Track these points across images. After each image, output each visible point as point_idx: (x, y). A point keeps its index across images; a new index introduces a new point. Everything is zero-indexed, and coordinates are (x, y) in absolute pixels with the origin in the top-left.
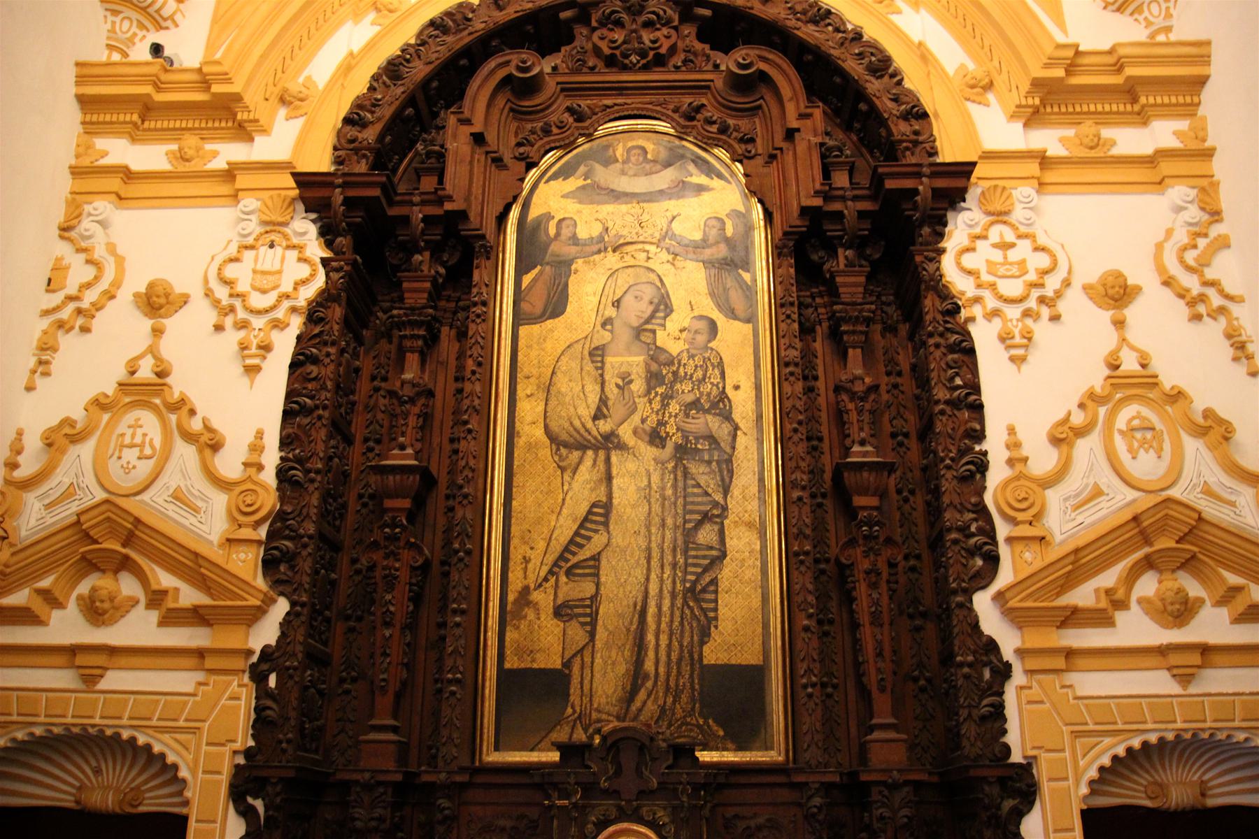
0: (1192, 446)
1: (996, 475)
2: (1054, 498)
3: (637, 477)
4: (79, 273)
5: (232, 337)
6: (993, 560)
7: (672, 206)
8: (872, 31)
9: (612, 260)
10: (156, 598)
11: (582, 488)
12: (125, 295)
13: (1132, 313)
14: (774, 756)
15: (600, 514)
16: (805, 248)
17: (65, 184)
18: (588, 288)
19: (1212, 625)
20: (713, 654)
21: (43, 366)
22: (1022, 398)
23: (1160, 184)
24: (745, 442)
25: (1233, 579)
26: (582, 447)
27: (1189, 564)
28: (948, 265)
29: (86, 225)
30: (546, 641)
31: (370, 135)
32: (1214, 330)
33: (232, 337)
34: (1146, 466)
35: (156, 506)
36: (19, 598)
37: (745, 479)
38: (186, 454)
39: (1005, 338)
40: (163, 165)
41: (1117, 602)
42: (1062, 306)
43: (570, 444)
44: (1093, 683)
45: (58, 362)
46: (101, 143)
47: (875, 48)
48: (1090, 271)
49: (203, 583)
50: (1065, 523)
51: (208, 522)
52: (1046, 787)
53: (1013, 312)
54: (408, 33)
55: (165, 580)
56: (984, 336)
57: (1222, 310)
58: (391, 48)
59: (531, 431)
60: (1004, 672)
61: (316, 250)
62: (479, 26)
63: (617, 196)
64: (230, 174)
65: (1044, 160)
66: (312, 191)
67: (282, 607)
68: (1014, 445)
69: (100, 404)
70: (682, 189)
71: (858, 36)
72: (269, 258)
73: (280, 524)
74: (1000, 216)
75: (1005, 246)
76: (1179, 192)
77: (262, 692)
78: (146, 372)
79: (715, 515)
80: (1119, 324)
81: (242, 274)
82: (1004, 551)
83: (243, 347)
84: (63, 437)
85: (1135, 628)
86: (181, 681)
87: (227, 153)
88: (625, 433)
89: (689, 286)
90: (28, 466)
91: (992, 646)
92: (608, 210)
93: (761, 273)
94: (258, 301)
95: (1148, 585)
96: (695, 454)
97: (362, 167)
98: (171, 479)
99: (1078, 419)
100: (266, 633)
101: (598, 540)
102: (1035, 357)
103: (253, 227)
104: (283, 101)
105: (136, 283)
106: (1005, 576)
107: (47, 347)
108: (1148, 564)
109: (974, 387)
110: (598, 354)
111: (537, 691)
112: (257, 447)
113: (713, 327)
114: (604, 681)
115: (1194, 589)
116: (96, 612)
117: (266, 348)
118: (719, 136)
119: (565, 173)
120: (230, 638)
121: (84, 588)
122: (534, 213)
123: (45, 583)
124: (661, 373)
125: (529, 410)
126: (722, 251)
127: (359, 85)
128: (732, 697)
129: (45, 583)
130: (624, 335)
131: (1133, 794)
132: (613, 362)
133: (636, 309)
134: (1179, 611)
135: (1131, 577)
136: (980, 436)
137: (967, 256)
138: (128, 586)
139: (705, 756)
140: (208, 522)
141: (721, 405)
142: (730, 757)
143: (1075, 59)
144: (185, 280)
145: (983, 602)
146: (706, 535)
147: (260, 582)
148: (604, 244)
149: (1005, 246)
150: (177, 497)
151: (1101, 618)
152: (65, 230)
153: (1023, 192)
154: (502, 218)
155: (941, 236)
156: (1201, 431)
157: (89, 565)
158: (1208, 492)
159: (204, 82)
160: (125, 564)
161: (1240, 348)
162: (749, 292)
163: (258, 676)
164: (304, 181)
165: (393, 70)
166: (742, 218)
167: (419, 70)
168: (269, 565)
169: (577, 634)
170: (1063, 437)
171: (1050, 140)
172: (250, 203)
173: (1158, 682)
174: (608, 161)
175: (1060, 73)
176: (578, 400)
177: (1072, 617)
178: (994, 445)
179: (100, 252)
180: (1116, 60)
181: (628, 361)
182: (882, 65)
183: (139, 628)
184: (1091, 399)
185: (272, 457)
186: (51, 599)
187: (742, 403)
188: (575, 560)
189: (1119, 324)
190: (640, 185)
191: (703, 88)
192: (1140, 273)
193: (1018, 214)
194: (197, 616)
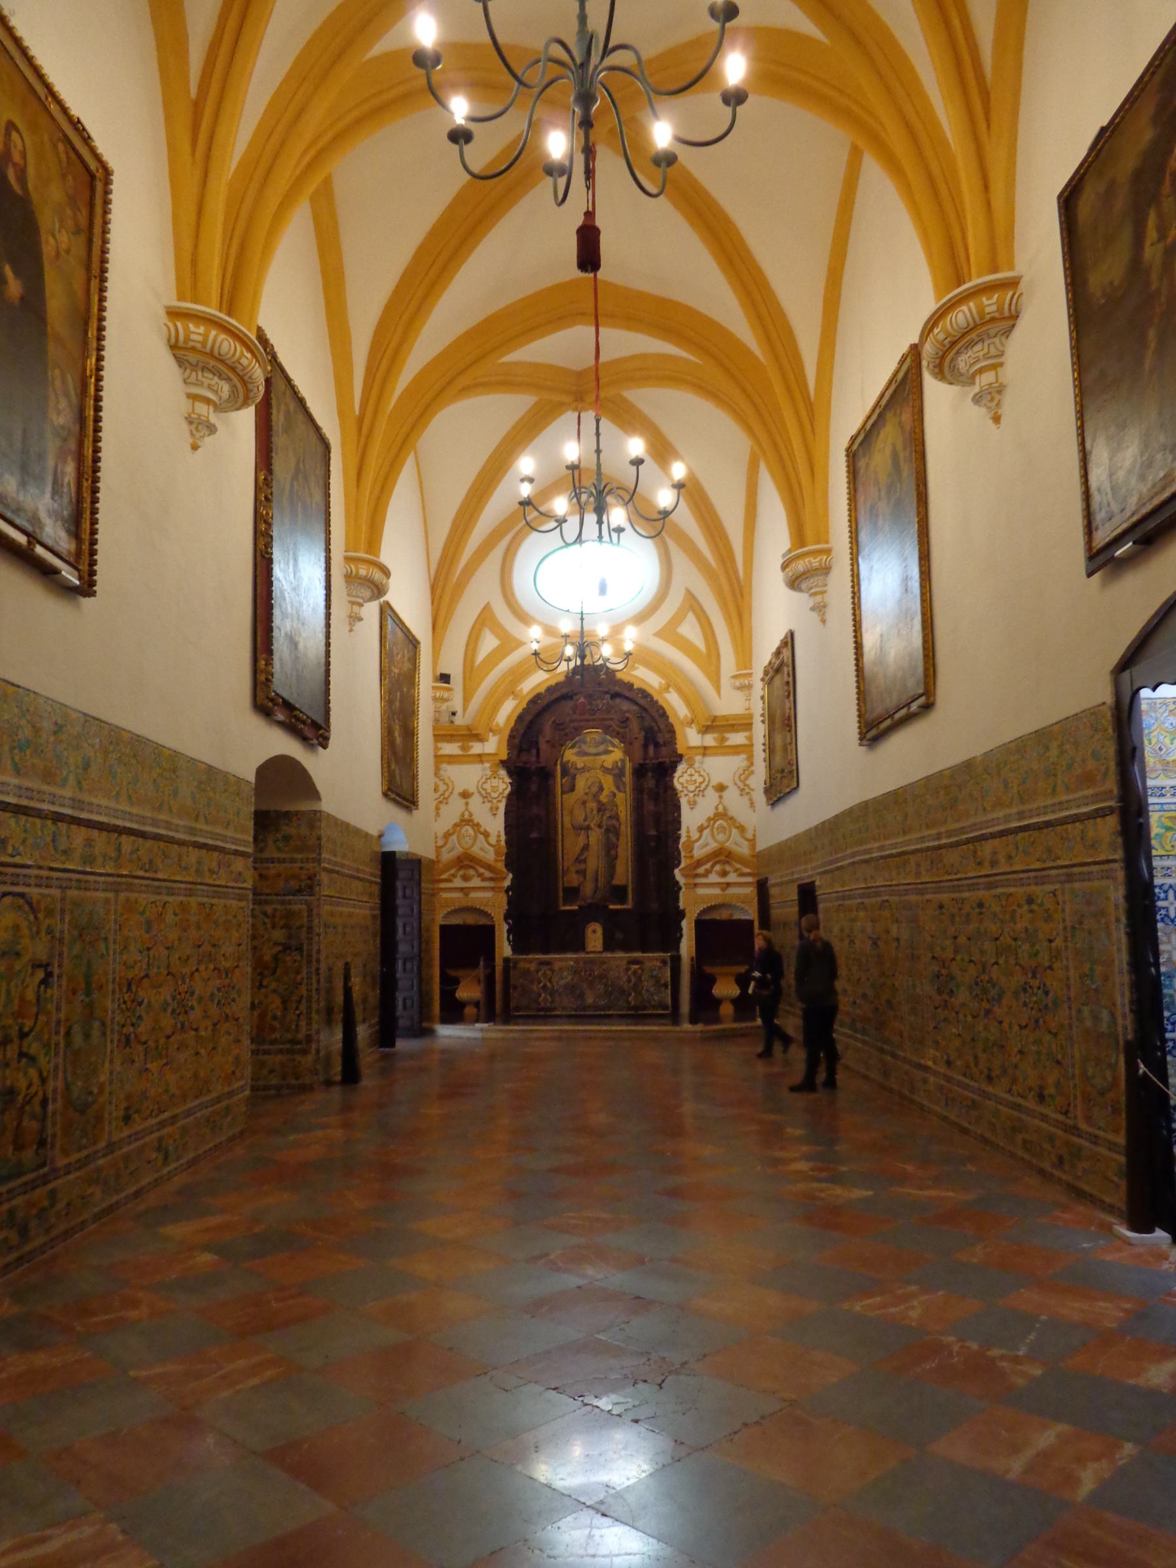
0: (734, 831)
1: (683, 839)
2: (696, 845)
3: (595, 837)
4: (442, 788)
5: (488, 805)
6: (680, 862)
7: (603, 757)
8: (661, 702)
9: (587, 774)
10: (480, 875)
11: (581, 841)
12: (456, 792)
13: (725, 794)
14: (629, 906)
15: (586, 847)
16: (640, 772)
17: (431, 760)
18: (581, 783)
19: (732, 878)
20: (615, 882)
21: (438, 815)
22: (691, 818)
23: (738, 753)
24: (623, 828)
25: (738, 866)
26: (581, 829)
27: (727, 862)
28: (675, 780)
29: (442, 772)
30: (573, 879)
31: (517, 741)
32: (746, 798)
33: (488, 805)
34: (721, 837)
35: (476, 851)
36: (444, 877)
37: (622, 840)
38: (481, 837)
39: (689, 802)
40: (460, 752)
41: (707, 873)
42: (706, 793)
43: (577, 828)
44: (701, 891)
45: (441, 812)
46: (440, 745)
47: (663, 708)
48: (714, 782)
49: (492, 871)
50: (698, 853)
51: (490, 856)
52: (688, 915)
53: (691, 795)
54: (524, 705)
55: (481, 870)
56: (684, 802)
57: (748, 793)
58: (520, 710)
59: (568, 824)
60: (680, 888)
61: (508, 780)
62: (544, 702)
63: (586, 754)
64: (479, 756)
65: (705, 748)
66: (503, 763)
67: (511, 876)
68: (688, 832)
69: (456, 825)
70: (607, 752)
71: (657, 702)
72: (495, 782)
73: (508, 856)
74: (691, 766)
75: (691, 775)
76: (744, 756)
77: (508, 896)
78: (467, 814)
79: (616, 847)
80: (721, 797)
81: (486, 786)
82: (683, 860)
83: (491, 808)
84: (447, 835)
85: (713, 878)
86: (489, 894)
87: (477, 748)
88: (592, 825)
89: (608, 782)
90: (440, 843)
91: (677, 882)
92: (585, 758)
93: (628, 778)
94: (495, 795)
95: (718, 868)
96: (612, 831)
97: (516, 752)
98: (478, 844)
99: (706, 824)
100: (507, 883)
101: (586, 854)
102: (697, 807)
103: (489, 773)
104: (491, 730)
105: (459, 789)
106: (682, 865)
107: (437, 809)
108: (717, 862)
109: (680, 816)
110: (584, 803)
111: (572, 893)
112: (499, 836)
113: (614, 795)
114: (588, 889)
115: (728, 868)
116: (466, 878)
117: (497, 808)
118: (617, 735)
119: (573, 747)
120: (499, 884)
121: (462, 872)
122: (565, 759)
123: (452, 872)
124: (601, 808)
125: (567, 819)
126: (617, 771)
127: (512, 724)
128: (619, 893)
129: (452, 872)
130: (591, 797)
131: (716, 916)
132: (589, 805)
133: (595, 789)
134: (724, 874)
135: (713, 867)
136: (679, 829)
137: (682, 778)
138: (471, 872)
139: (611, 907)
140: (490, 856)
141: (616, 817)
142: (619, 907)
143: (715, 718)
144: (472, 789)
145: (676, 871)
146: (613, 852)
147: (505, 870)
148: (584, 769)
149: (691, 775)
150: (481, 849)
151: (706, 875)
152: (437, 773)
153: (698, 758)
154: (556, 764)
155: (674, 771)
156: (737, 828)
157: (461, 868)
158: (736, 843)
159: (468, 728)
160: (471, 867)
161: (752, 804)
162: (624, 783)
163: (507, 891)
164: (503, 762)
165: (520, 718)
166: (623, 761)
167: (529, 718)
168: (506, 866)
169: (582, 879)
170: (701, 829)
171: (710, 740)
172: (487, 765)
173: (717, 891)
174: (585, 743)
175: (709, 723)
176: (580, 816)
177: (697, 876)
178: (683, 832)
179: (447, 781)
180: (725, 718)
181: (593, 805)
182: (664, 715)
183: (476, 882)
184: (709, 819)
185: (503, 838)
186: (454, 876)
187: (622, 816)
188: (580, 860)
189: (721, 797)
190: (593, 750)
191: (611, 719)
192: (727, 781)
193: (697, 765)
194: (491, 879)
